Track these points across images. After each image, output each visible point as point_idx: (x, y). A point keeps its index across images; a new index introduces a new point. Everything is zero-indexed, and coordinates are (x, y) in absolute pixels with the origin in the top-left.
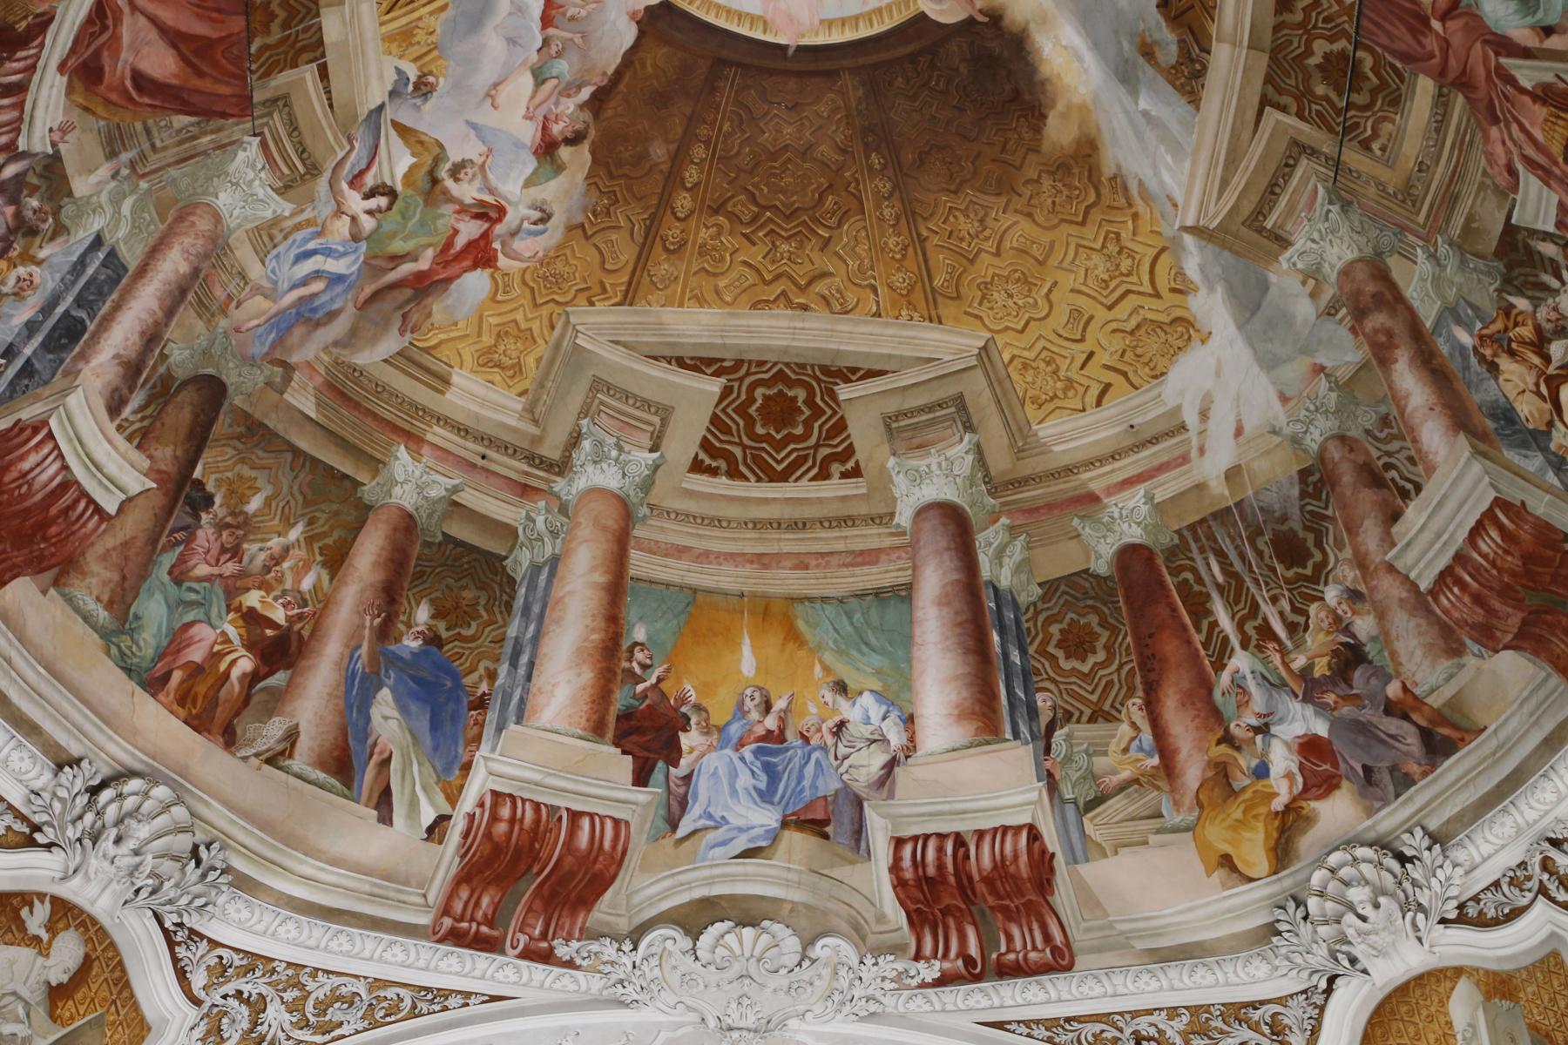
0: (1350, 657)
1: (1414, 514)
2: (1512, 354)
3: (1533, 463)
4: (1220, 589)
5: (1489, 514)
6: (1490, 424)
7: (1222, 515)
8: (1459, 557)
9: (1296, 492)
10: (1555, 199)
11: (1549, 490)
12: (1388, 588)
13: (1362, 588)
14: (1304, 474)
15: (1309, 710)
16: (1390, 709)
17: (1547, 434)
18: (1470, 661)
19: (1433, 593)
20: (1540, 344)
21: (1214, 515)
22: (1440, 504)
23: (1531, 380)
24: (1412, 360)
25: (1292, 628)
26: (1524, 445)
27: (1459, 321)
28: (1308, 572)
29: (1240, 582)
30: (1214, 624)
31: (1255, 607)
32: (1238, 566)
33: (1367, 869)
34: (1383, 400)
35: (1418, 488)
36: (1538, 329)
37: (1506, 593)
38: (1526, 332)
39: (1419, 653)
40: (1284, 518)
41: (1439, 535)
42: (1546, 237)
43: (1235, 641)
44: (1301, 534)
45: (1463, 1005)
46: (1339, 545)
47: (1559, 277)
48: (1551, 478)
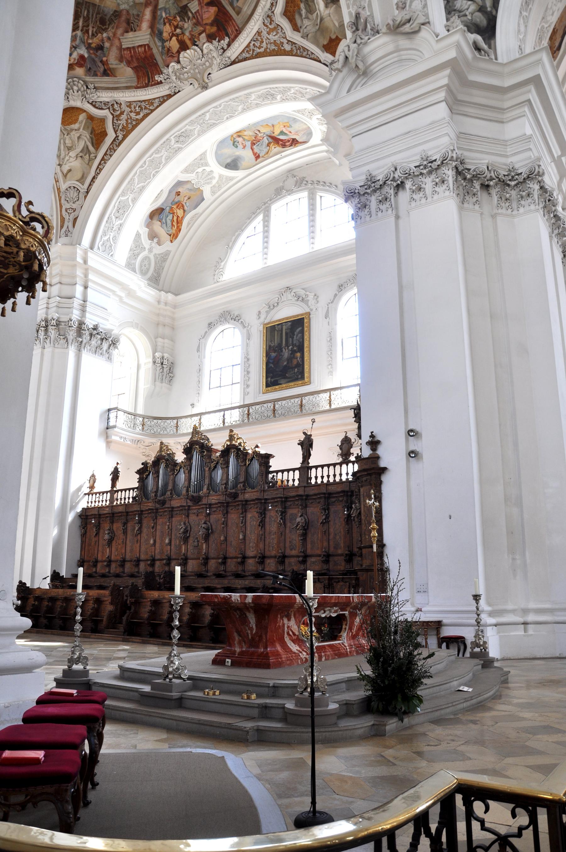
0: (100, 48)
1: (131, 34)
2: (170, 25)
3: (159, 44)
4: (84, 17)
5: (145, 45)
6: (157, 32)
7: (94, 5)
8: (134, 48)
9: (112, 13)
10: (198, 8)
11: (158, 50)
12: (116, 42)
13: (111, 38)
14: (115, 11)
15: (86, 51)
16: (102, 61)
17: (165, 42)
18: (122, 65)
19: (124, 49)
20: (176, 27)
21: (93, 4)
22: (137, 37)
23: (170, 31)
24: (151, 10)
25: (93, 35)
26: (160, 40)
27: (165, 12)
28: (103, 28)
29: (89, 19)
30: (78, 23)
31: (88, 26)
32: (90, 16)
33: (80, 85)
34: (141, 12)
35: (135, 31)
36: (178, 25)
37: (137, 59)
38: (175, 23)
39: (113, 57)
40: (106, 15)
41: (133, 41)
42: (192, 12)
43: (80, 28)
44: (107, 20)
45: (82, 117)
46: (113, 28)
47: (188, 20)
48: (160, 48)
